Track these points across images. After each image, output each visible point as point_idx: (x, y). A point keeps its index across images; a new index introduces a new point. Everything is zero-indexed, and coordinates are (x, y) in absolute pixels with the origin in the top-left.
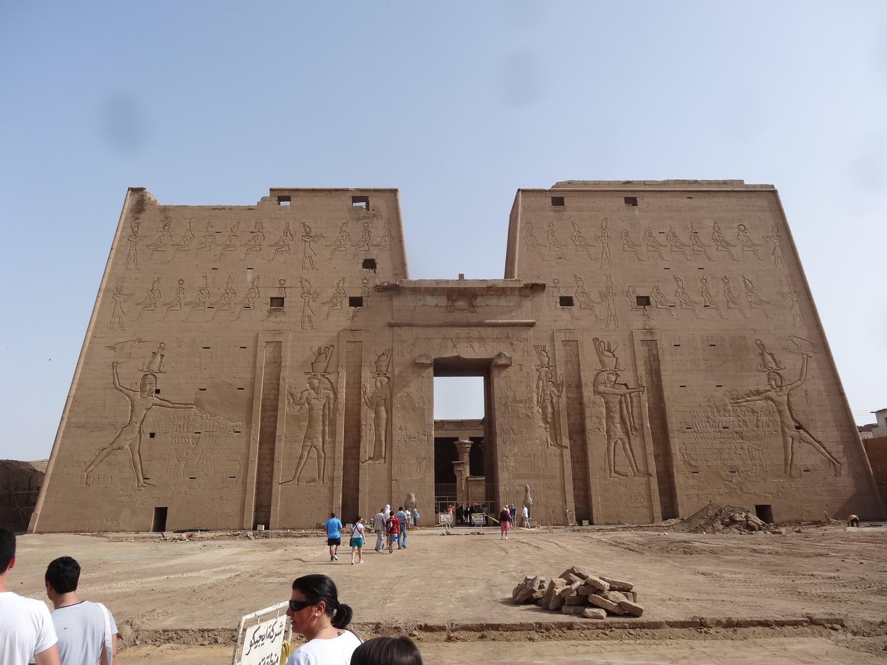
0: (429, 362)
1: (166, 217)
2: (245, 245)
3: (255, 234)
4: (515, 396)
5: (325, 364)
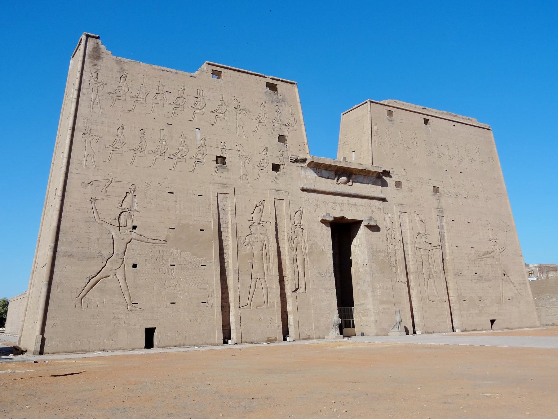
0: (331, 219)
1: (122, 70)
2: (191, 107)
3: (198, 100)
4: (377, 248)
5: (260, 214)
